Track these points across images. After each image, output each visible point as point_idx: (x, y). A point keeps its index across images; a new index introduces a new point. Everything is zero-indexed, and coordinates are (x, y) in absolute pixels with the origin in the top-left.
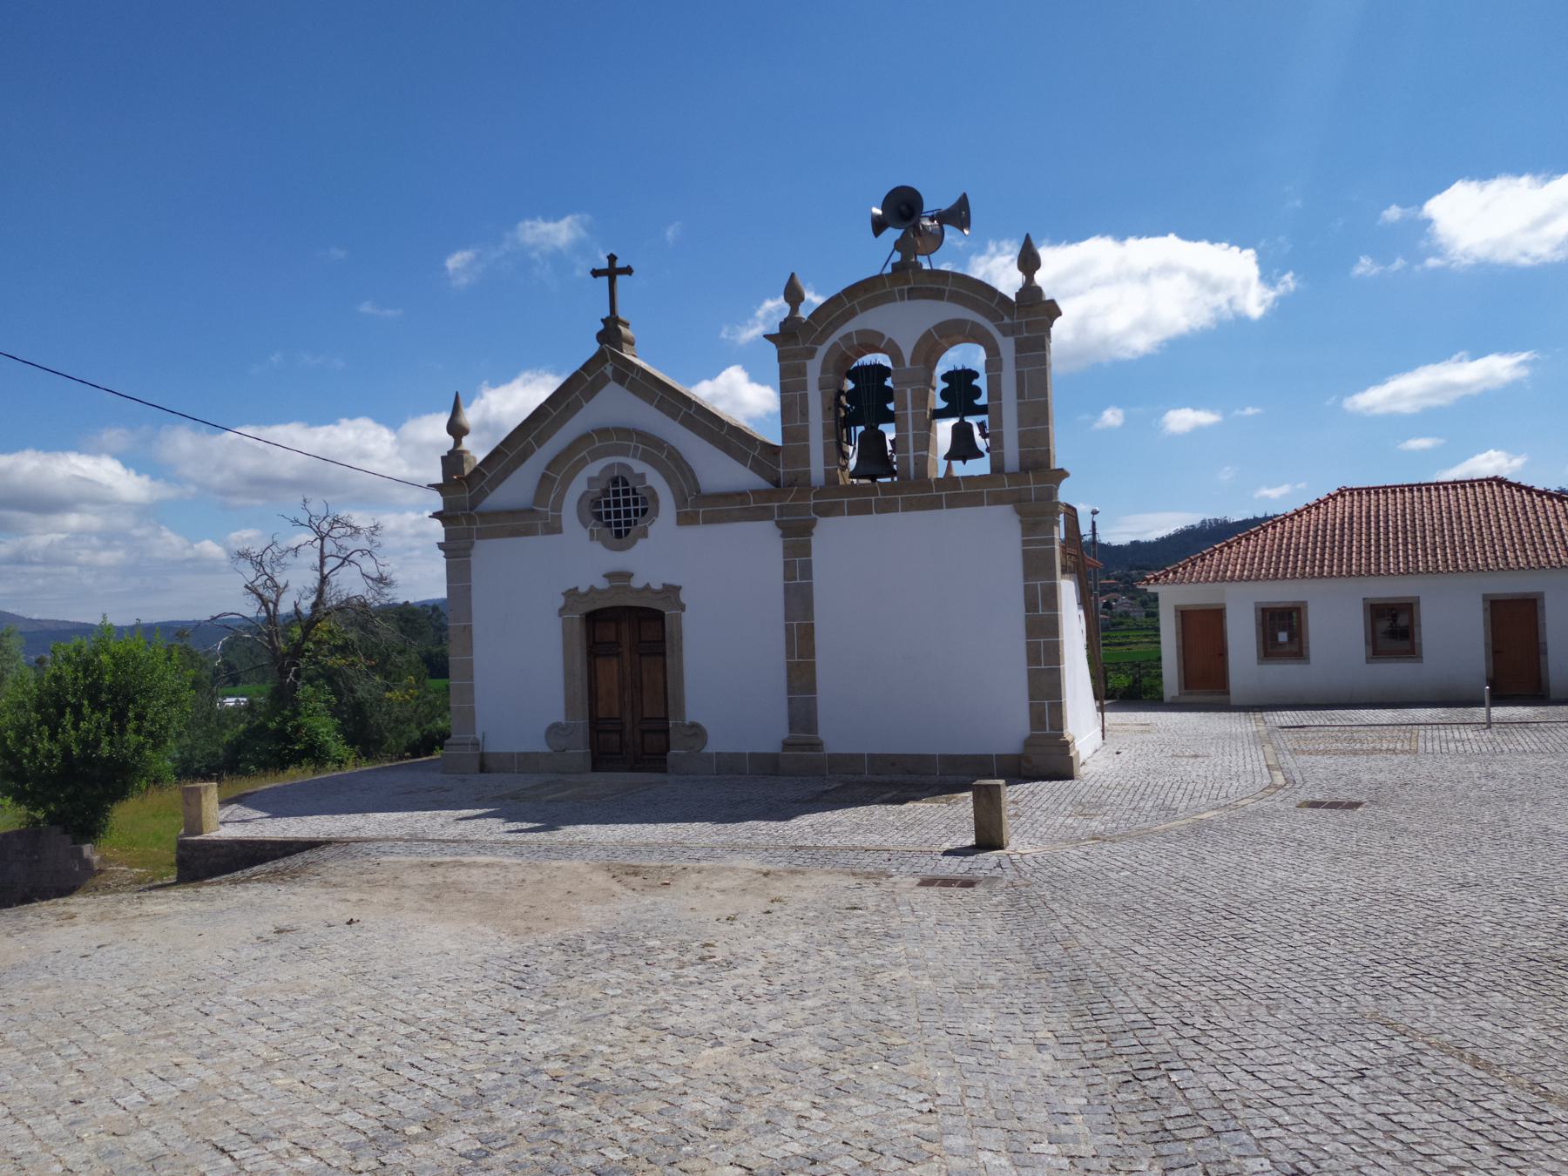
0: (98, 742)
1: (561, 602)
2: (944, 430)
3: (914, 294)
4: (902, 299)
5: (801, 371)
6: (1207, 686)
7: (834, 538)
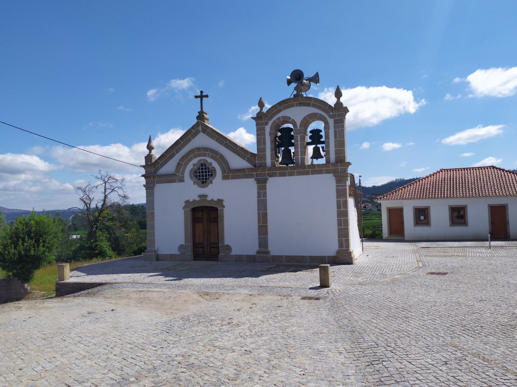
0: (30, 250)
1: (184, 205)
2: (310, 149)
3: (300, 104)
4: (297, 106)
5: (264, 129)
6: (397, 234)
7: (274, 184)
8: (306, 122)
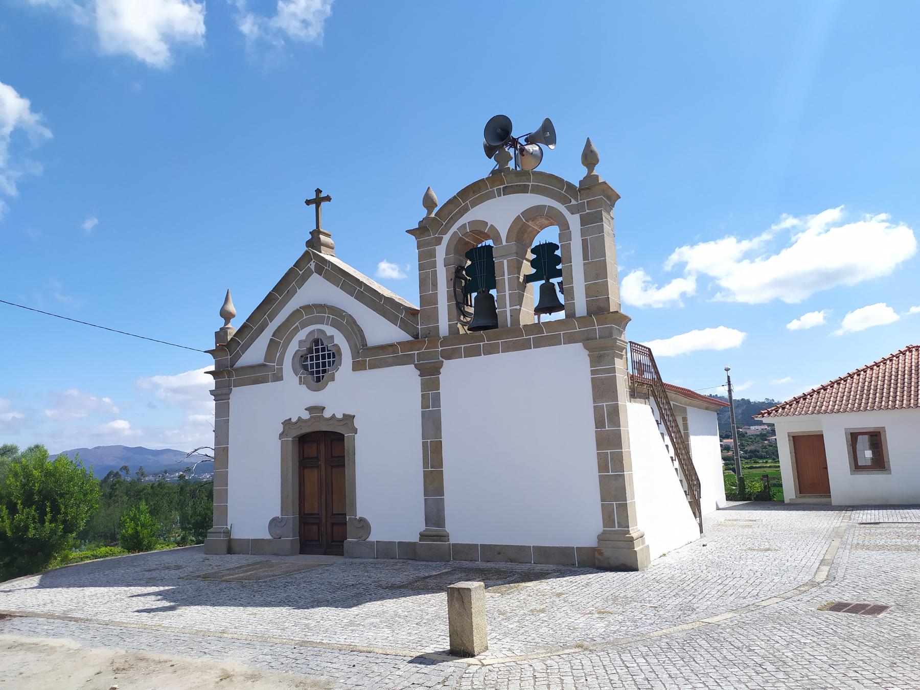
0: (26, 528)
1: (280, 429)
2: (533, 292)
3: (507, 191)
4: (499, 195)
5: (432, 254)
6: (814, 490)
7: (456, 373)
8: (522, 230)
